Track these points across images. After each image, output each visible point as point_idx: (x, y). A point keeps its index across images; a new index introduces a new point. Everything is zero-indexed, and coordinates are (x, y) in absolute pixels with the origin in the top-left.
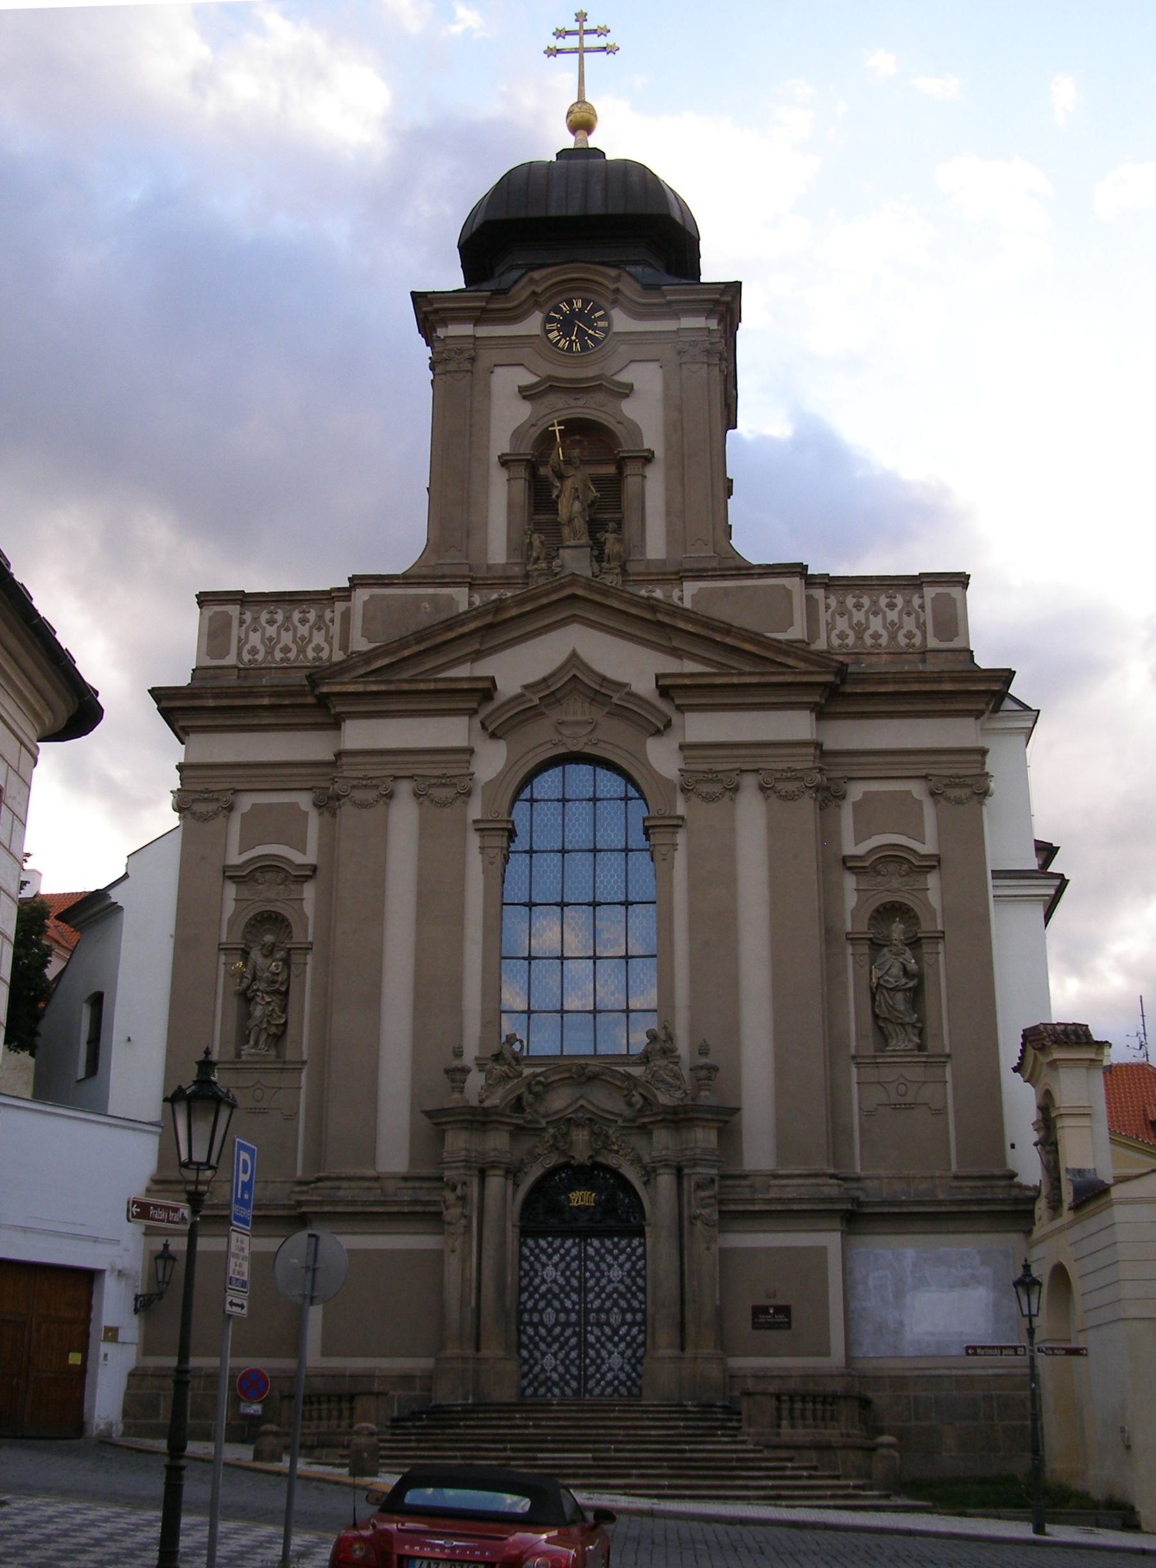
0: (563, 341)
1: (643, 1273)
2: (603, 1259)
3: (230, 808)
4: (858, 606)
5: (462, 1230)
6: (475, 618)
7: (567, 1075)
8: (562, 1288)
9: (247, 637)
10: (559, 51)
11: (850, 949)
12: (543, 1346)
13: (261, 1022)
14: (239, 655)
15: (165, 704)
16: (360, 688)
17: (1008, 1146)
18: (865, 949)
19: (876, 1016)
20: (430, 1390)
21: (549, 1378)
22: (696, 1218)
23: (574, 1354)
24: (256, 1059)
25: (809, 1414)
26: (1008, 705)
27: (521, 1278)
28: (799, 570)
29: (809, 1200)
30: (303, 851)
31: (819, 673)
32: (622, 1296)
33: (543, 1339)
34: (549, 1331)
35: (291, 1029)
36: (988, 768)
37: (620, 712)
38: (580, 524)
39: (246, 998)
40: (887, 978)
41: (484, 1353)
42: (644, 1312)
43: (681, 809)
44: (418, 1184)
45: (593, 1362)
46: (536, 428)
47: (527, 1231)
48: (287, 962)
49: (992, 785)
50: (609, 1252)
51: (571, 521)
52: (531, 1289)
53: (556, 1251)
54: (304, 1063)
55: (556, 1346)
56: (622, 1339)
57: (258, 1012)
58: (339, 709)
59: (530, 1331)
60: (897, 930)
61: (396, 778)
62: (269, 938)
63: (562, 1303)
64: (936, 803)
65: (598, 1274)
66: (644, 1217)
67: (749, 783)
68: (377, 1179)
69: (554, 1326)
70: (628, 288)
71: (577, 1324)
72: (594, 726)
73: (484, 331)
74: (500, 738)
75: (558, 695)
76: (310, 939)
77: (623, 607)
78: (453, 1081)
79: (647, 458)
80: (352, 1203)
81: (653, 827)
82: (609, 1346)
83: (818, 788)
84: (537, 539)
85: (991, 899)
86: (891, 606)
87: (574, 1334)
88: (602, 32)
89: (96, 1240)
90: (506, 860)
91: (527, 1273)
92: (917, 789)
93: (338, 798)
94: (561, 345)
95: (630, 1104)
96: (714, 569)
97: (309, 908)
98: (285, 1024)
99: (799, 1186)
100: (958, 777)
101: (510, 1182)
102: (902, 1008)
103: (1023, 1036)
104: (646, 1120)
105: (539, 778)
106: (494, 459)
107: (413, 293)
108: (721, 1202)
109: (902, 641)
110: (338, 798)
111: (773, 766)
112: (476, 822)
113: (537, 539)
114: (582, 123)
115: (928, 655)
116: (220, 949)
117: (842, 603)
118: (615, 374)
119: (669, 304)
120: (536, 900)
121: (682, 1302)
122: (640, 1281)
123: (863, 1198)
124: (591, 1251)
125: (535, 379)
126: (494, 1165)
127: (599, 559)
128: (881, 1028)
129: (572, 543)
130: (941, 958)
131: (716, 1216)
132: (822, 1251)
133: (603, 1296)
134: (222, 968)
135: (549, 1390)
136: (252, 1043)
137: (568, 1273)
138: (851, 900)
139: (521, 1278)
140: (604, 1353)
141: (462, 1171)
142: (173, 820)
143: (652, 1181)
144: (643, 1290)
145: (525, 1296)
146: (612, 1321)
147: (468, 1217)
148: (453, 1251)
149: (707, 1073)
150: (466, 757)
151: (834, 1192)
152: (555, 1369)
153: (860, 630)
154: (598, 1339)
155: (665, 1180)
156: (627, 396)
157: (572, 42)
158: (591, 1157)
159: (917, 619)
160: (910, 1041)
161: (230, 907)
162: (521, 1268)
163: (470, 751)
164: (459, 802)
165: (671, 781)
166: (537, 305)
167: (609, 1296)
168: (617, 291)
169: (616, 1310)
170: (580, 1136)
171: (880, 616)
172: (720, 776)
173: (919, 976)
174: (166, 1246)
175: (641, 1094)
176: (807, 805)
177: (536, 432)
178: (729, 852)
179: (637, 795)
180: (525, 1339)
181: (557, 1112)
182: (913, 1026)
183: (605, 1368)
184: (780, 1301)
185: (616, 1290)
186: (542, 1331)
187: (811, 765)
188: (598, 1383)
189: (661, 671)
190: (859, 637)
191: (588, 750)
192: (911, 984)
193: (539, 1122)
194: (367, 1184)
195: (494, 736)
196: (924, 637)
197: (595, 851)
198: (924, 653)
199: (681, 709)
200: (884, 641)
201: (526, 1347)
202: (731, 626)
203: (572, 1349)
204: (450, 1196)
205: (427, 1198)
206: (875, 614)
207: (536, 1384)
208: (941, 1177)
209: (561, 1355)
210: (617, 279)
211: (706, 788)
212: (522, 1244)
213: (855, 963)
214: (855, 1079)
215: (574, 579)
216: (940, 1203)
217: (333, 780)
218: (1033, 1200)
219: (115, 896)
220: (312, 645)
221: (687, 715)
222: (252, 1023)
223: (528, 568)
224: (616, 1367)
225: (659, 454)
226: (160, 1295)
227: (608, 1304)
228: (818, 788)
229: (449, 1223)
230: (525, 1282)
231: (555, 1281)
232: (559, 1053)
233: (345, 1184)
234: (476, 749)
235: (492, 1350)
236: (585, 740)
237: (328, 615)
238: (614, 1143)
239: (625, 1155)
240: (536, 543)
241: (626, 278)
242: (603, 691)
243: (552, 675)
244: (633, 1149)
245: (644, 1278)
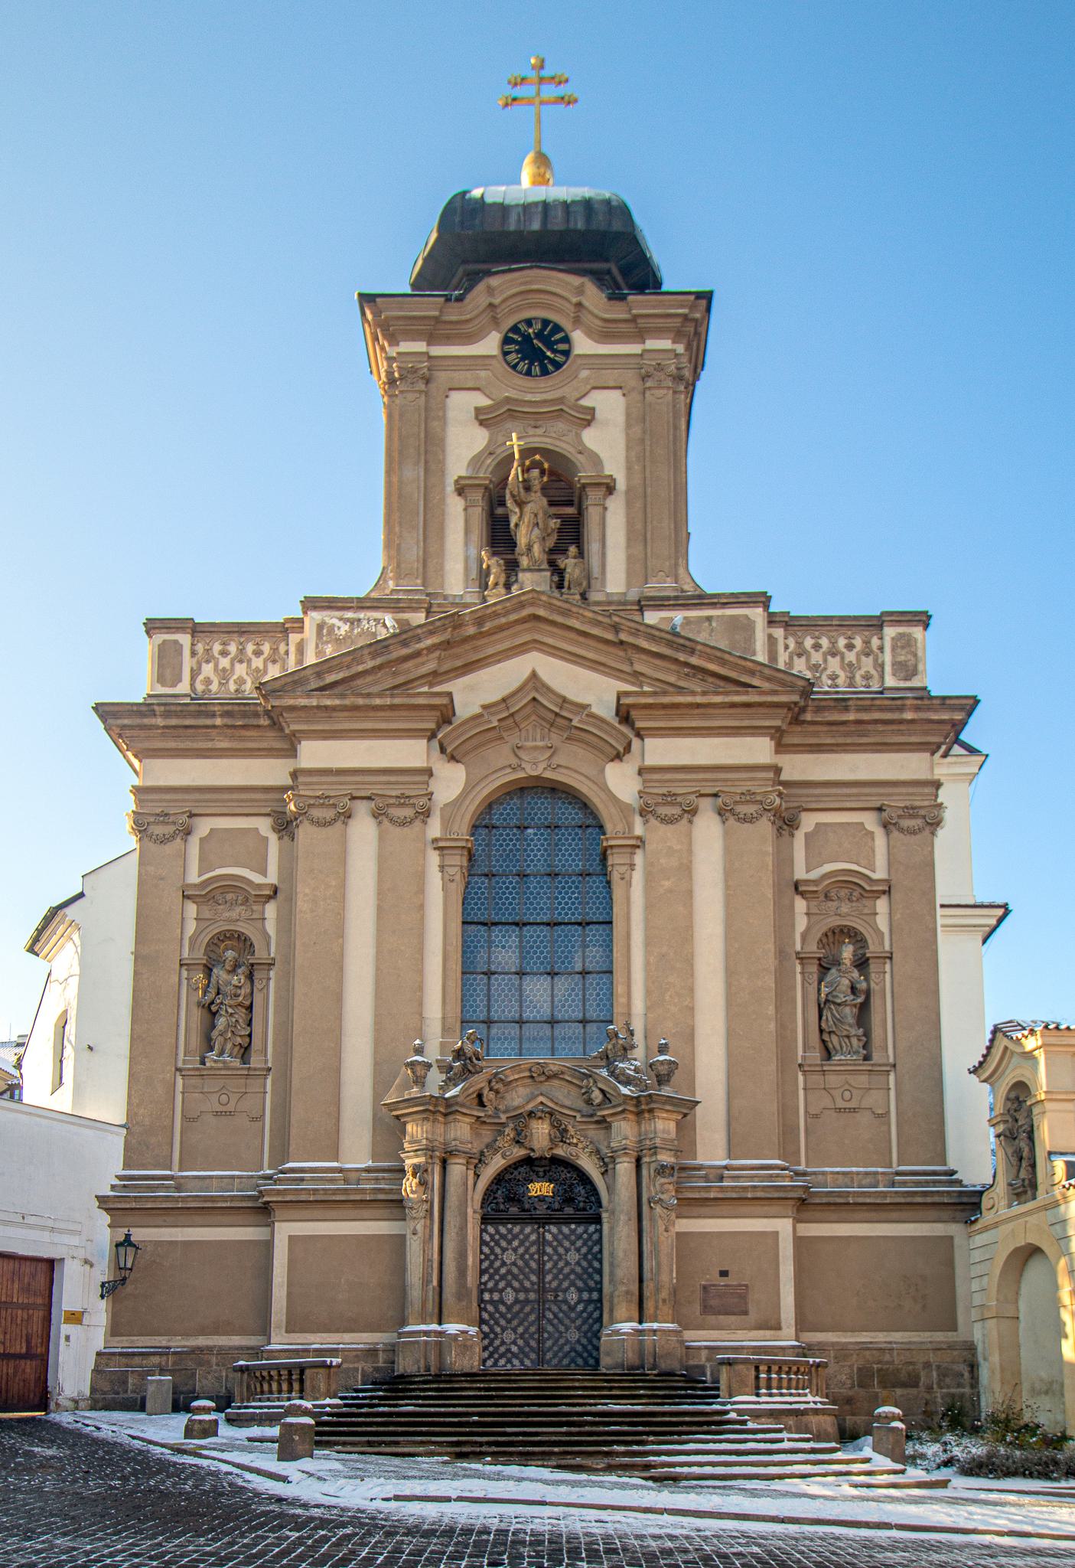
0: (522, 364)
1: (599, 1256)
3: (188, 832)
5: (423, 1214)
13: (226, 1031)
20: (393, 1362)
21: (509, 1350)
27: (481, 1261)
30: (264, 873)
33: (503, 1316)
39: (211, 1012)
42: (600, 1291)
43: (639, 830)
46: (492, 457)
47: (485, 1220)
48: (250, 977)
50: (566, 1237)
52: (491, 1271)
53: (515, 1237)
54: (270, 1069)
55: (515, 1323)
57: (221, 1022)
59: (490, 1308)
61: (353, 798)
63: (521, 1284)
65: (555, 1258)
66: (600, 1204)
74: (458, 762)
75: (517, 718)
76: (272, 955)
91: (487, 1257)
94: (519, 368)
96: (676, 598)
97: (271, 927)
98: (250, 1035)
100: (913, 808)
101: (471, 1173)
102: (851, 1020)
106: (450, 488)
111: (733, 789)
112: (435, 840)
116: (181, 965)
122: (596, 1264)
124: (549, 1237)
127: (560, 586)
130: (888, 977)
133: (561, 1277)
134: (185, 982)
135: (509, 1361)
137: (527, 1256)
142: (132, 842)
143: (610, 1172)
144: (600, 1272)
145: (485, 1278)
150: (426, 778)
156: (588, 423)
161: (191, 927)
162: (481, 1252)
163: (429, 772)
164: (418, 823)
167: (567, 1277)
169: (572, 1289)
172: (679, 799)
173: (868, 993)
176: (765, 827)
180: (485, 1316)
185: (573, 1271)
186: (502, 1309)
188: (555, 1355)
191: (548, 775)
192: (860, 1000)
193: (499, 1117)
195: (453, 758)
203: (531, 1324)
209: (521, 1330)
211: (663, 811)
212: (482, 1231)
213: (804, 980)
222: (215, 1034)
225: (621, 485)
230: (486, 1264)
231: (514, 1264)
236: (544, 765)
245: (600, 1261)
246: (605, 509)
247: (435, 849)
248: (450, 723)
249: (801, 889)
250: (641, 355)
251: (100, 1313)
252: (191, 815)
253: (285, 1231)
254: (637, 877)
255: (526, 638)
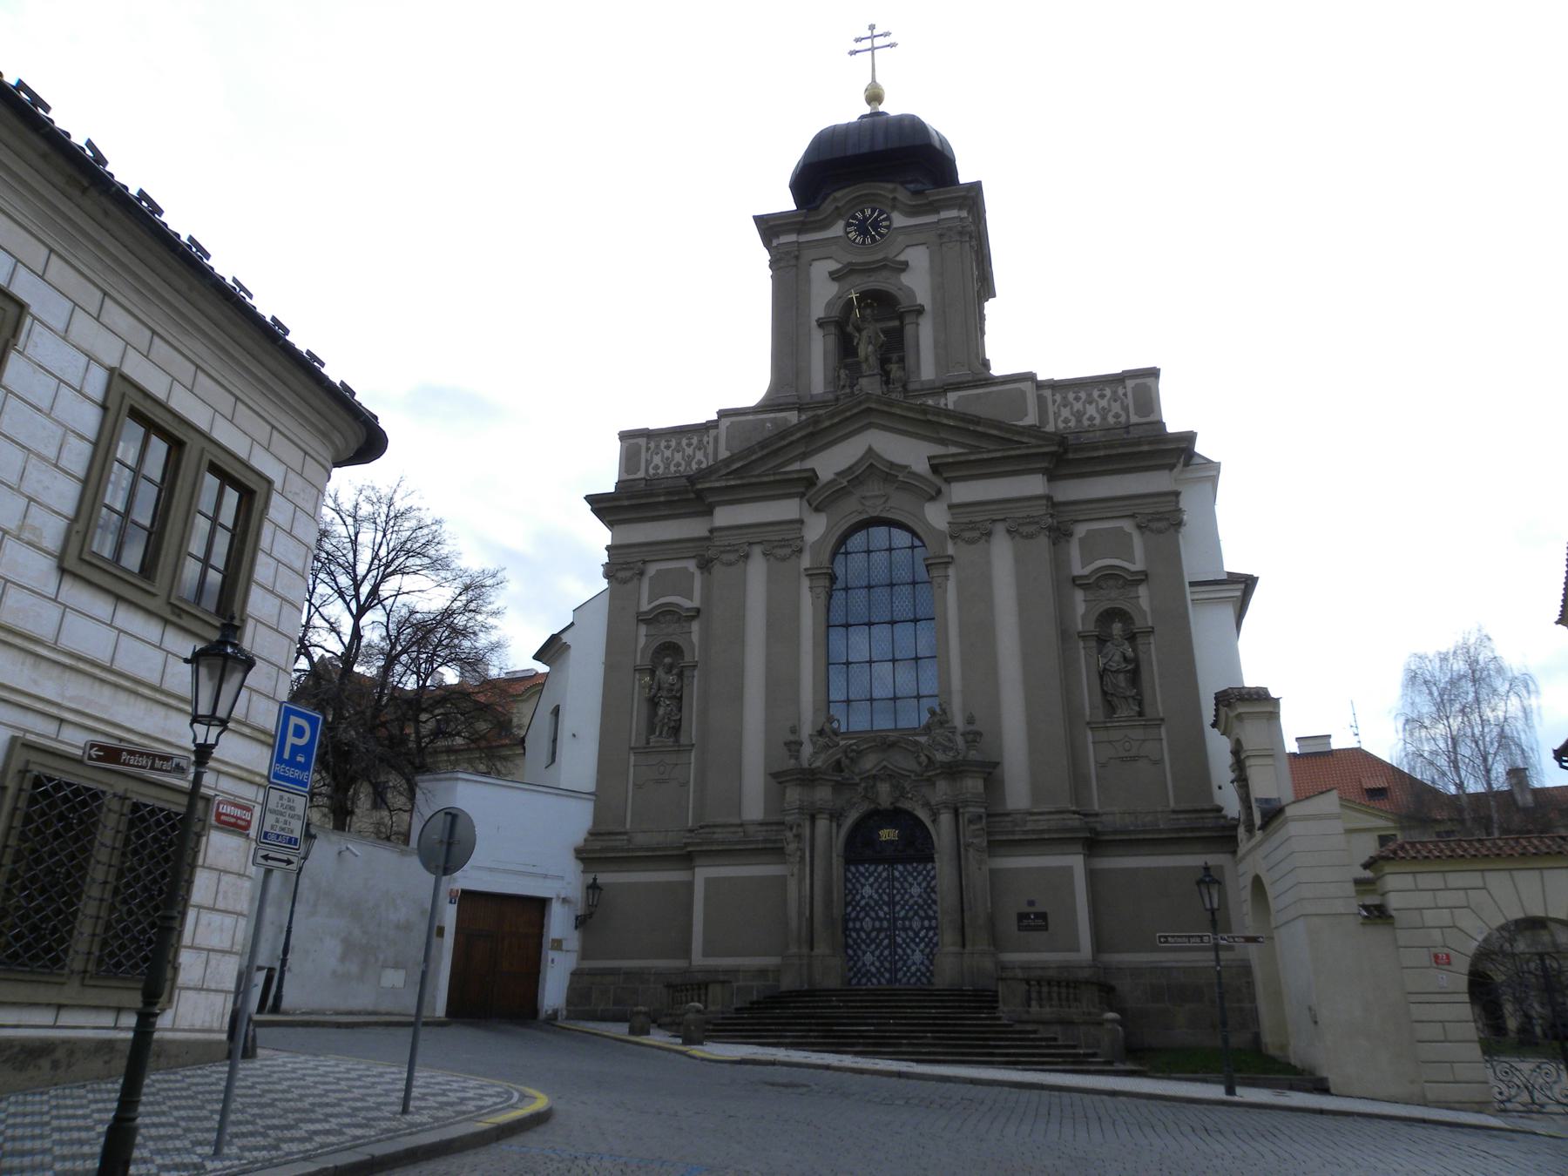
2: (906, 880)
3: (642, 574)
4: (1077, 399)
6: (800, 429)
7: (873, 744)
8: (876, 902)
9: (652, 457)
10: (857, 52)
11: (1081, 644)
12: (863, 946)
13: (664, 718)
14: (647, 471)
15: (596, 506)
16: (723, 484)
17: (1215, 788)
18: (1093, 644)
19: (1105, 693)
21: (869, 971)
22: (968, 845)
23: (886, 953)
24: (659, 744)
25: (1055, 995)
26: (1196, 460)
27: (846, 895)
28: (1029, 377)
29: (1056, 831)
30: (690, 598)
31: (1047, 446)
32: (921, 907)
34: (868, 935)
35: (684, 724)
36: (1182, 505)
37: (905, 487)
38: (872, 360)
39: (653, 703)
40: (1111, 663)
41: (817, 951)
42: (936, 919)
43: (951, 550)
44: (769, 828)
45: (901, 958)
48: (680, 675)
49: (1185, 517)
51: (867, 359)
52: (854, 903)
53: (871, 874)
54: (693, 745)
55: (873, 946)
56: (922, 940)
57: (661, 711)
58: (710, 500)
59: (854, 935)
60: (1117, 628)
61: (750, 544)
62: (668, 660)
63: (877, 914)
64: (1143, 533)
65: (902, 891)
66: (933, 848)
67: (1000, 529)
68: (741, 825)
69: (871, 931)
70: (902, 195)
71: (888, 929)
72: (887, 498)
73: (804, 238)
77: (904, 413)
78: (790, 750)
79: (920, 311)
80: (723, 843)
81: (931, 564)
82: (912, 945)
83: (1050, 529)
84: (843, 373)
85: (1189, 602)
86: (1102, 396)
87: (886, 937)
88: (886, 34)
89: (545, 876)
90: (830, 597)
91: (850, 891)
92: (1127, 525)
93: (711, 560)
95: (920, 764)
96: (968, 382)
97: (695, 638)
98: (680, 719)
99: (1049, 820)
100: (1158, 513)
101: (834, 825)
102: (1123, 684)
103: (1216, 698)
104: (930, 774)
105: (853, 538)
106: (814, 324)
107: (754, 217)
108: (989, 834)
109: (1111, 420)
110: (711, 560)
112: (805, 570)
113: (843, 373)
114: (874, 96)
115: (1131, 428)
117: (1065, 398)
118: (896, 256)
119: (931, 203)
120: (851, 621)
121: (962, 911)
123: (1099, 827)
124: (897, 874)
125: (840, 266)
126: (821, 811)
127: (887, 382)
128: (1109, 702)
129: (868, 373)
130: (1152, 646)
131: (985, 844)
132: (1068, 870)
134: (637, 683)
135: (869, 980)
136: (657, 733)
137: (880, 891)
138: (1081, 608)
139: (846, 895)
140: (909, 951)
141: (797, 816)
142: (603, 584)
145: (850, 909)
146: (914, 926)
147: (802, 850)
148: (792, 875)
149: (973, 737)
150: (799, 526)
151: (1077, 823)
152: (873, 964)
153: (1079, 415)
154: (904, 940)
155: (946, 818)
156: (903, 270)
157: (867, 44)
158: (892, 804)
159: (1122, 403)
160: (1132, 709)
161: (642, 641)
162: (846, 888)
163: (801, 522)
165: (944, 532)
166: (840, 216)
167: (911, 908)
168: (894, 199)
169: (916, 918)
170: (884, 788)
171: (1094, 405)
172: (978, 525)
173: (1136, 661)
174: (595, 879)
175: (926, 756)
176: (1043, 541)
177: (841, 303)
178: (987, 580)
179: (921, 544)
181: (868, 771)
182: (1133, 697)
183: (910, 962)
184: (1038, 908)
185: (916, 903)
186: (863, 935)
187: (1044, 512)
188: (905, 975)
189: (932, 454)
190: (1079, 421)
191: (884, 515)
192: (1129, 667)
193: (853, 779)
194: (733, 829)
195: (817, 510)
196: (1128, 416)
197: (892, 585)
198: (1127, 427)
199: (948, 481)
200: (1097, 421)
201: (851, 947)
202: (980, 418)
203: (885, 948)
204: (789, 835)
205: (774, 838)
206: (1090, 403)
207: (859, 975)
208: (1162, 812)
209: (877, 953)
210: (894, 190)
211: (967, 535)
212: (846, 870)
214: (1090, 738)
215: (869, 396)
216: (1160, 831)
217: (708, 548)
218: (1235, 827)
219: (565, 638)
220: (696, 460)
221: (952, 484)
222: (657, 720)
223: (839, 393)
224: (918, 962)
225: (928, 307)
226: (590, 915)
227: (911, 914)
228: (1050, 529)
229: (789, 855)
230: (849, 898)
231: (871, 897)
232: (869, 729)
233: (719, 830)
234: (805, 520)
235: (821, 949)
236: (879, 508)
237: (705, 439)
238: (908, 793)
239: (917, 801)
240: (843, 376)
241: (900, 188)
242: (892, 472)
243: (856, 463)
244: (923, 796)
246: (918, 324)
247: (807, 575)
248: (815, 484)
249: (1078, 582)
250: (938, 222)
251: (573, 940)
252: (645, 562)
253: (703, 874)
254: (951, 586)
255: (866, 421)
